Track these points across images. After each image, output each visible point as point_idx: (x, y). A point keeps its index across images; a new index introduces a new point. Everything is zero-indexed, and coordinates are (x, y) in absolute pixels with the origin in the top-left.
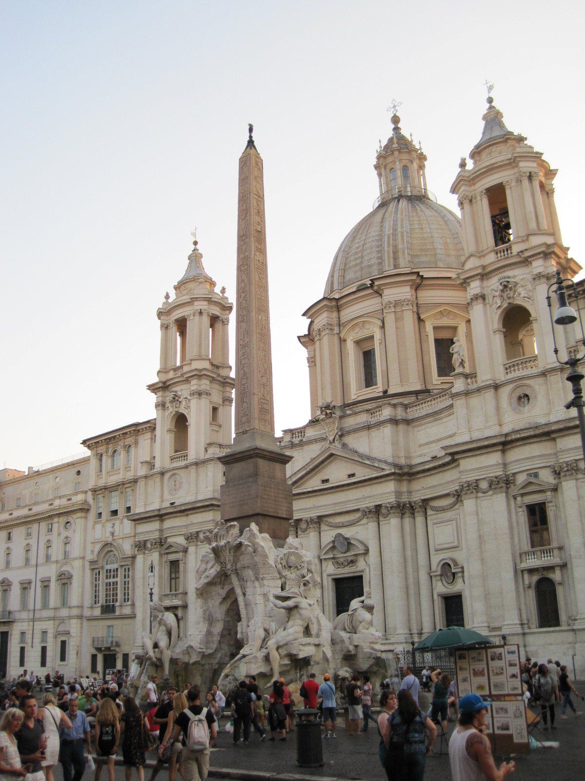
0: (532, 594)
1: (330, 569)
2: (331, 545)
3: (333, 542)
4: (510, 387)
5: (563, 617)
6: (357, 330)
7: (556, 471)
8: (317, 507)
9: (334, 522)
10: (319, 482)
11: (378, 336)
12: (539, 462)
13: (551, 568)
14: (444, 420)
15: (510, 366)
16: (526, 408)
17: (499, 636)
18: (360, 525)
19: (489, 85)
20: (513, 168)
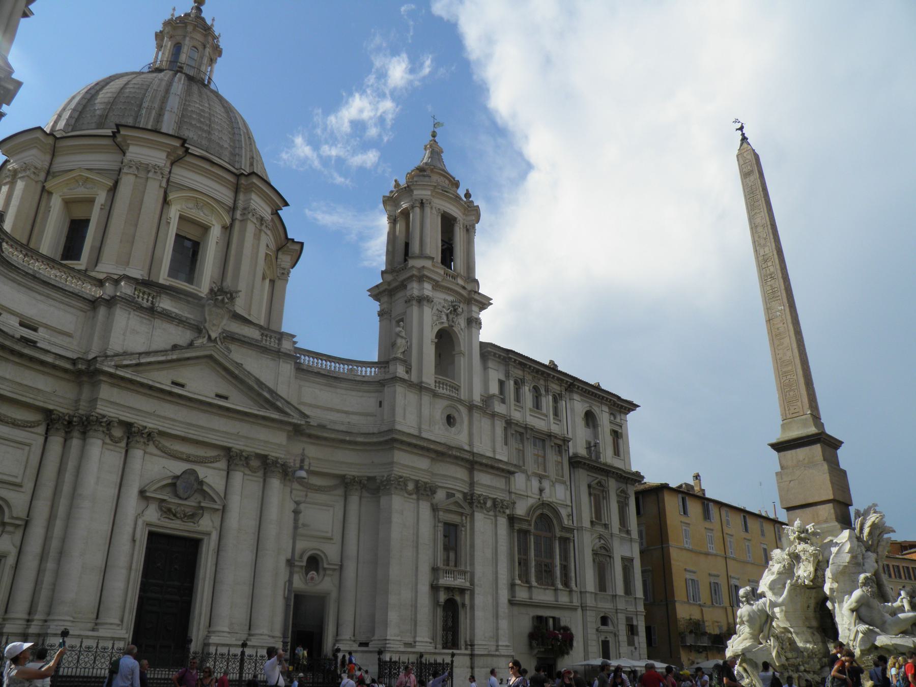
0: (440, 612)
1: (152, 515)
2: (170, 481)
3: (177, 477)
4: (446, 403)
5: (462, 643)
6: (191, 205)
7: (472, 499)
8: (159, 416)
9: (172, 447)
10: (169, 383)
11: (216, 232)
12: (460, 485)
13: (462, 591)
14: (338, 390)
15: (439, 382)
16: (453, 429)
17: (414, 653)
18: (214, 468)
19: (436, 121)
20: (464, 214)
